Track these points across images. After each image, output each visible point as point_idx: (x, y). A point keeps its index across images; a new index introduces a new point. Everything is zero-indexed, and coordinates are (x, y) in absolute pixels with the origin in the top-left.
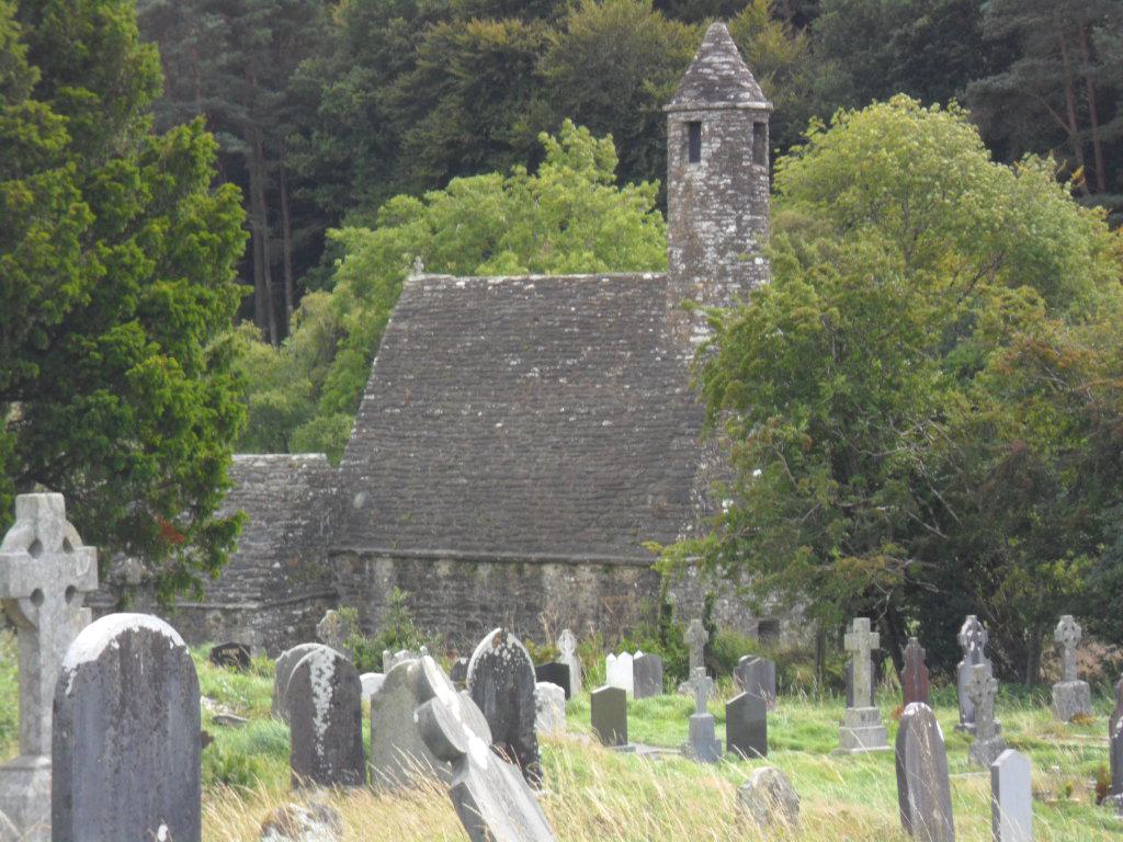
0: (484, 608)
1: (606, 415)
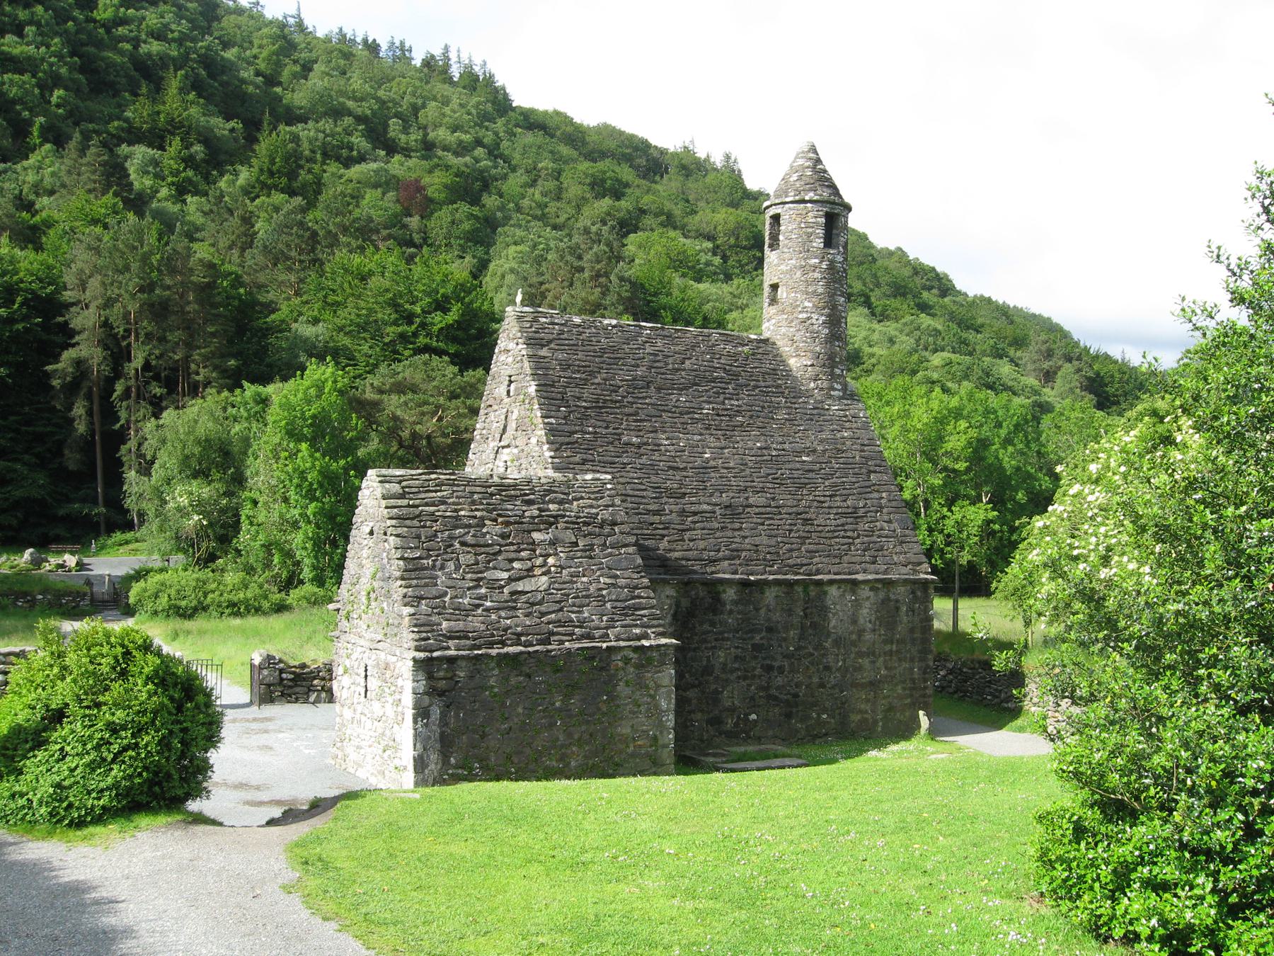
0: (770, 630)
1: (799, 453)
